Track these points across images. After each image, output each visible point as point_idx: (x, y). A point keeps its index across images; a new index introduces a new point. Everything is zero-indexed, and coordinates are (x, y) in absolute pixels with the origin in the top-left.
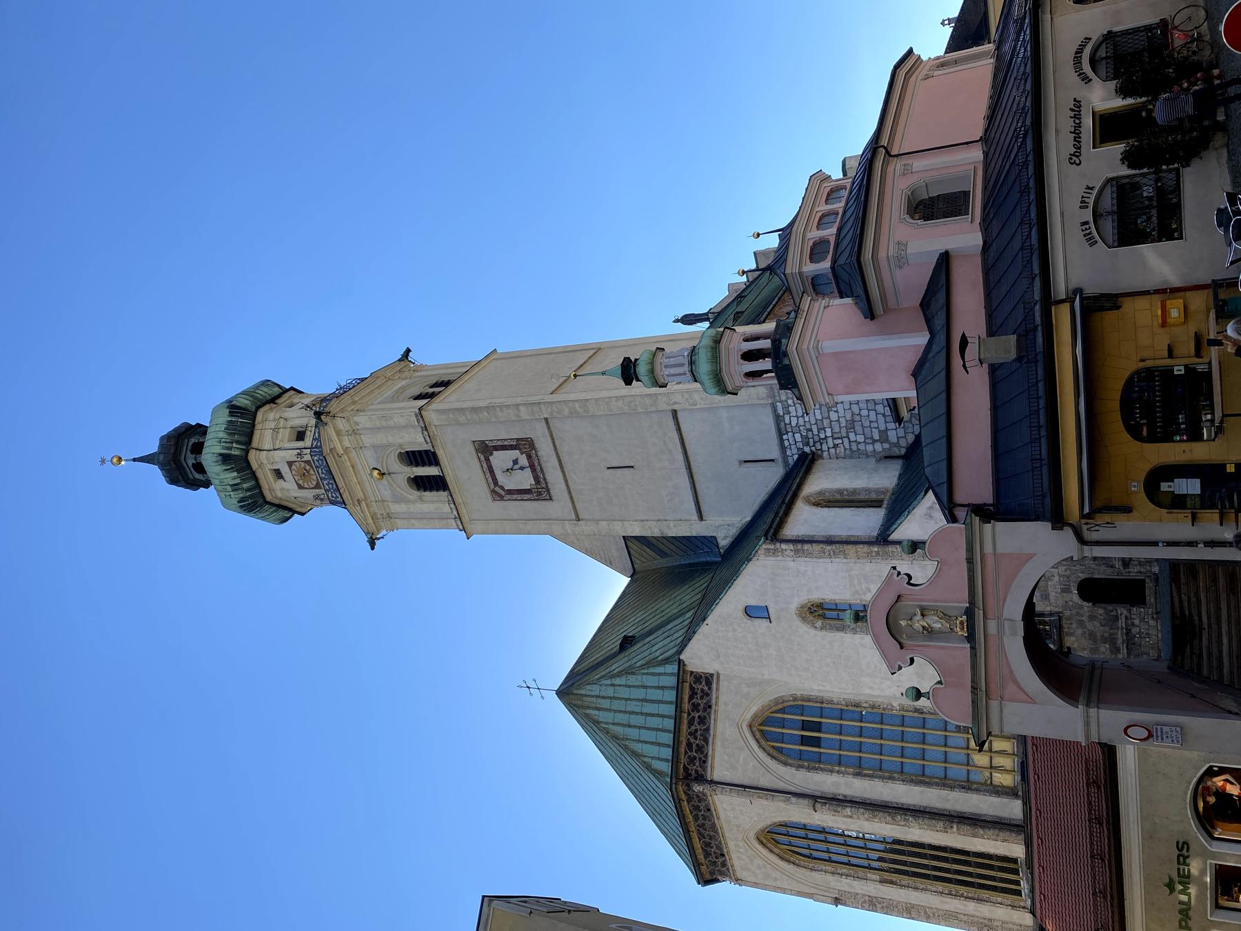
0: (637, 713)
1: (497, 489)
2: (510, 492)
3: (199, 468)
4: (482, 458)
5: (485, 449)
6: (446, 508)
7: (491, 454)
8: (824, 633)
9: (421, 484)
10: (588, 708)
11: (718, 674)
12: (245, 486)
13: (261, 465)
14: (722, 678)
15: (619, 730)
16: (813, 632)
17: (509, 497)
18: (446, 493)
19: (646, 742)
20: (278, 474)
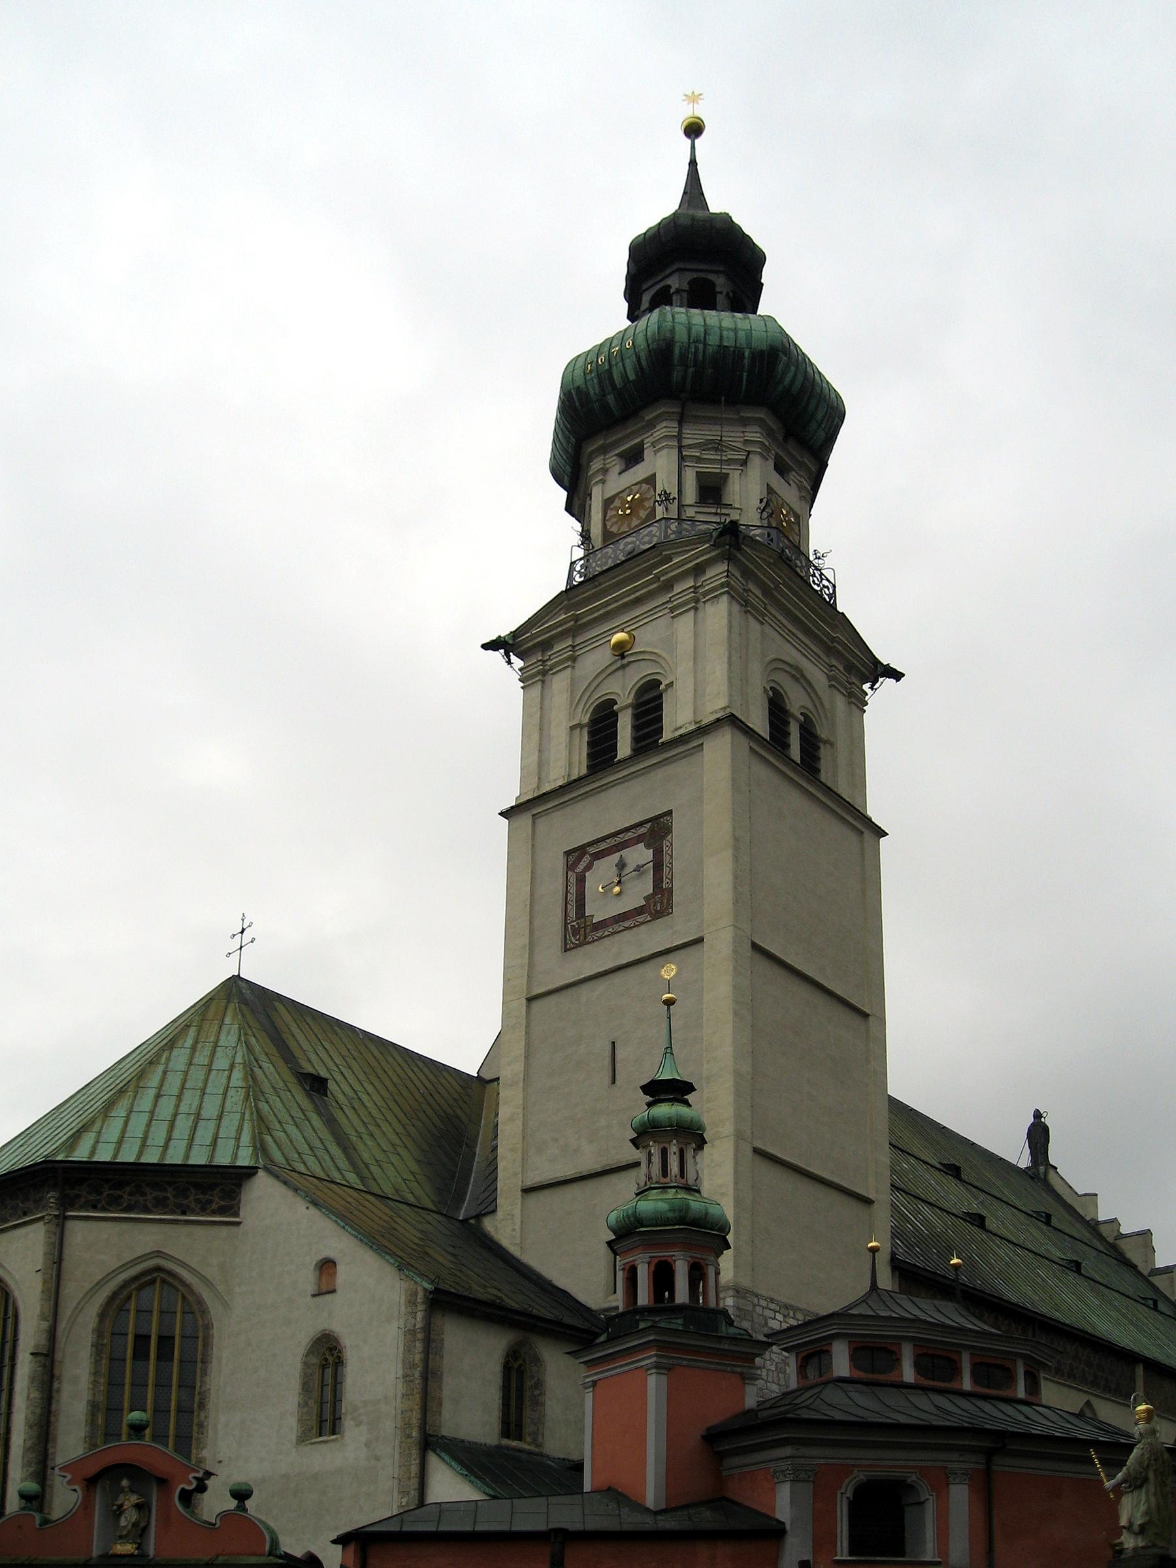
0: (177, 1106)
3: (663, 298)
4: (643, 830)
6: (556, 777)
7: (648, 847)
8: (298, 1365)
9: (601, 726)
11: (238, 1224)
12: (610, 398)
13: (651, 425)
14: (233, 1229)
16: (301, 1351)
18: (584, 771)
19: (126, 1124)
20: (633, 457)
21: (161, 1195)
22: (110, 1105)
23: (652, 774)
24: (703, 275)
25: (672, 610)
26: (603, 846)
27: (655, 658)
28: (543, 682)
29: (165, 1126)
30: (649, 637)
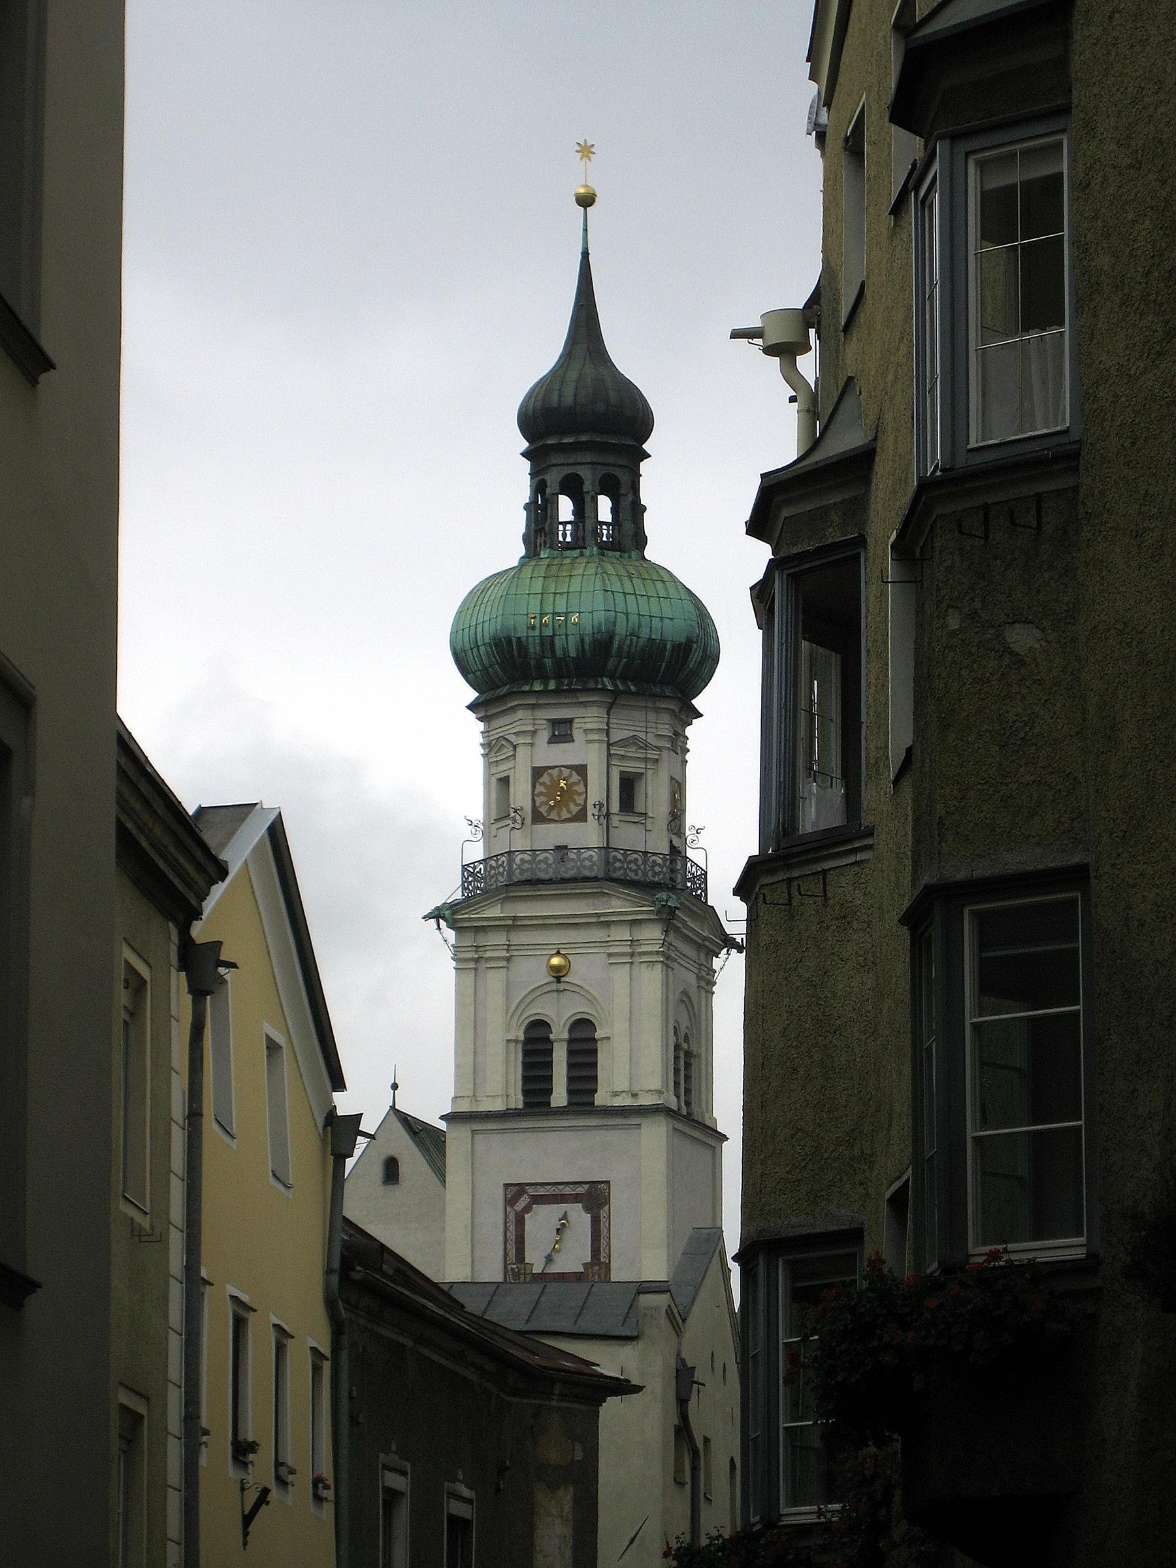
2: (520, 1222)
5: (595, 1197)
7: (587, 1209)
9: (535, 1044)
17: (512, 1216)
20: (561, 732)
23: (592, 1133)
24: (611, 470)
26: (542, 1191)
27: (592, 1001)
28: (476, 969)
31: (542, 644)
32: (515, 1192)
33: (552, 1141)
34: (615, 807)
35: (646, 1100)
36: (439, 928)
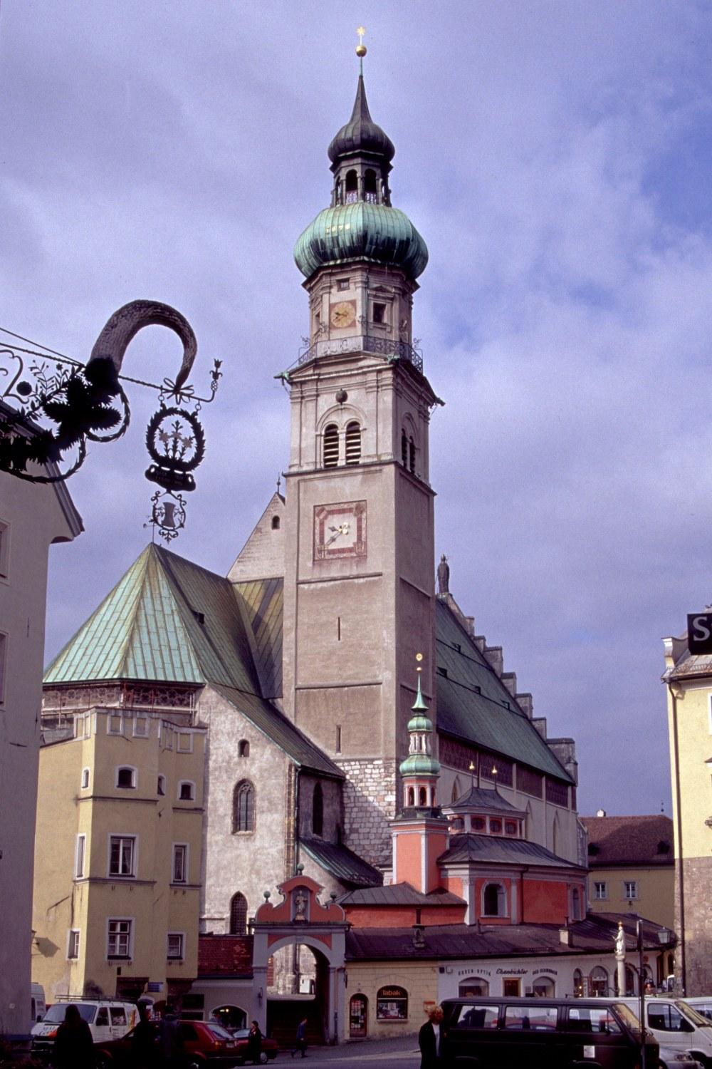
1: (325, 513)
2: (322, 524)
5: (359, 509)
7: (355, 515)
10: (150, 584)
12: (336, 250)
15: (143, 623)
21: (164, 696)
22: (131, 640)
24: (371, 168)
25: (366, 389)
26: (333, 508)
29: (158, 653)
30: (352, 396)
31: (333, 241)
32: (319, 510)
33: (337, 483)
34: (371, 320)
35: (384, 458)
36: (283, 384)
